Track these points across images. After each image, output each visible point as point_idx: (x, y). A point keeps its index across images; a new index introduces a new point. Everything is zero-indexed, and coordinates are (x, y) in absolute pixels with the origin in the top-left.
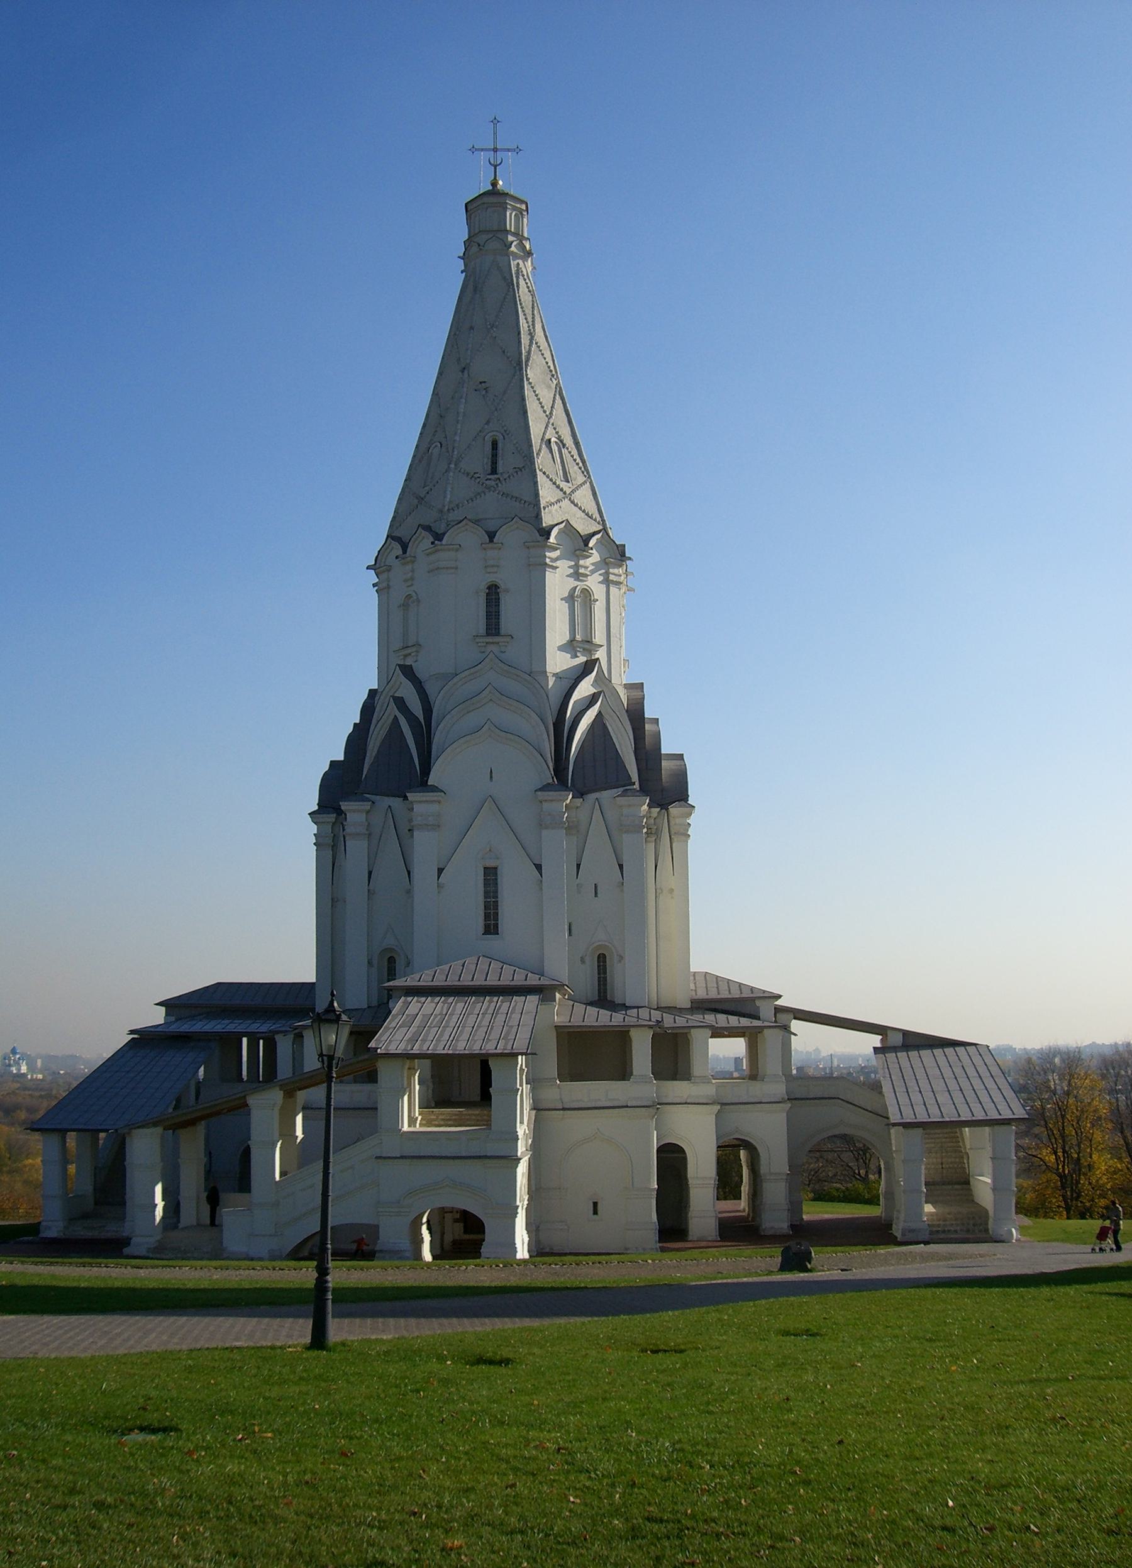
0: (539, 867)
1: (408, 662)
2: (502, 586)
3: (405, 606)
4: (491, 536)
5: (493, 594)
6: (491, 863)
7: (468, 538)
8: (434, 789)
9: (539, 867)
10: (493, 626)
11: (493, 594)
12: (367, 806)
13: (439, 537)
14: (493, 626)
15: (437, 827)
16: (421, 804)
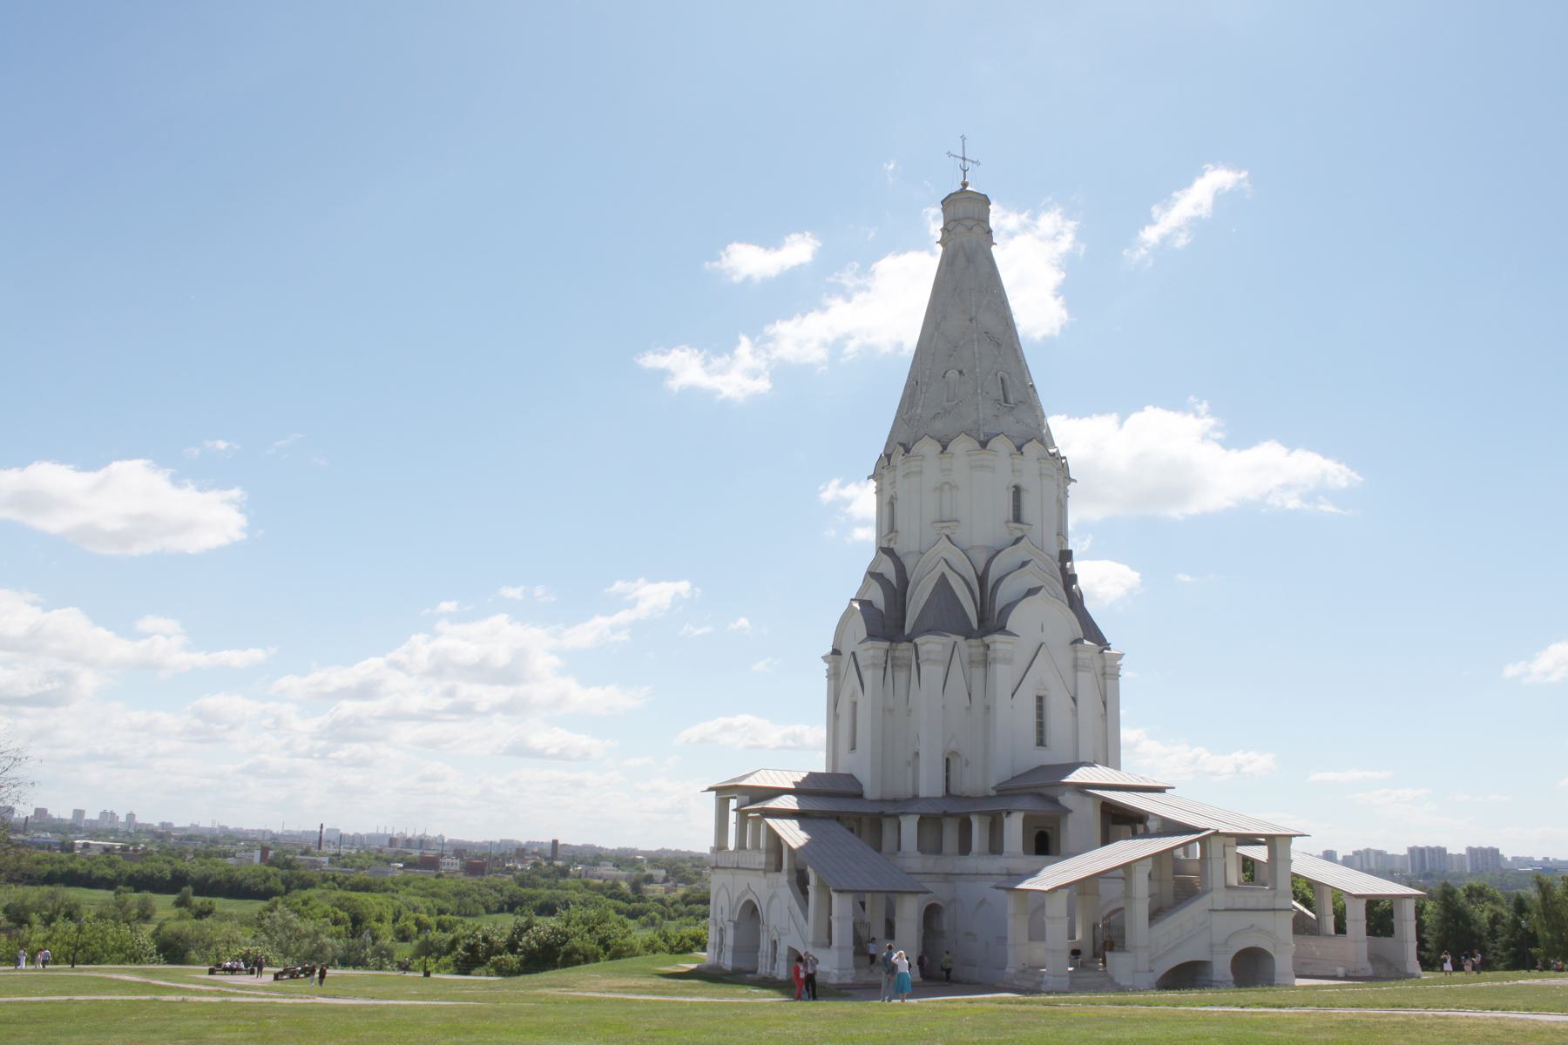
0: (1074, 699)
1: (947, 532)
2: (1023, 485)
3: (940, 489)
4: (1019, 448)
5: (1017, 491)
6: (1041, 693)
7: (1001, 446)
8: (1010, 634)
9: (1074, 699)
10: (1017, 518)
11: (1017, 491)
12: (943, 640)
13: (984, 445)
14: (1017, 518)
15: (1009, 661)
16: (998, 642)
